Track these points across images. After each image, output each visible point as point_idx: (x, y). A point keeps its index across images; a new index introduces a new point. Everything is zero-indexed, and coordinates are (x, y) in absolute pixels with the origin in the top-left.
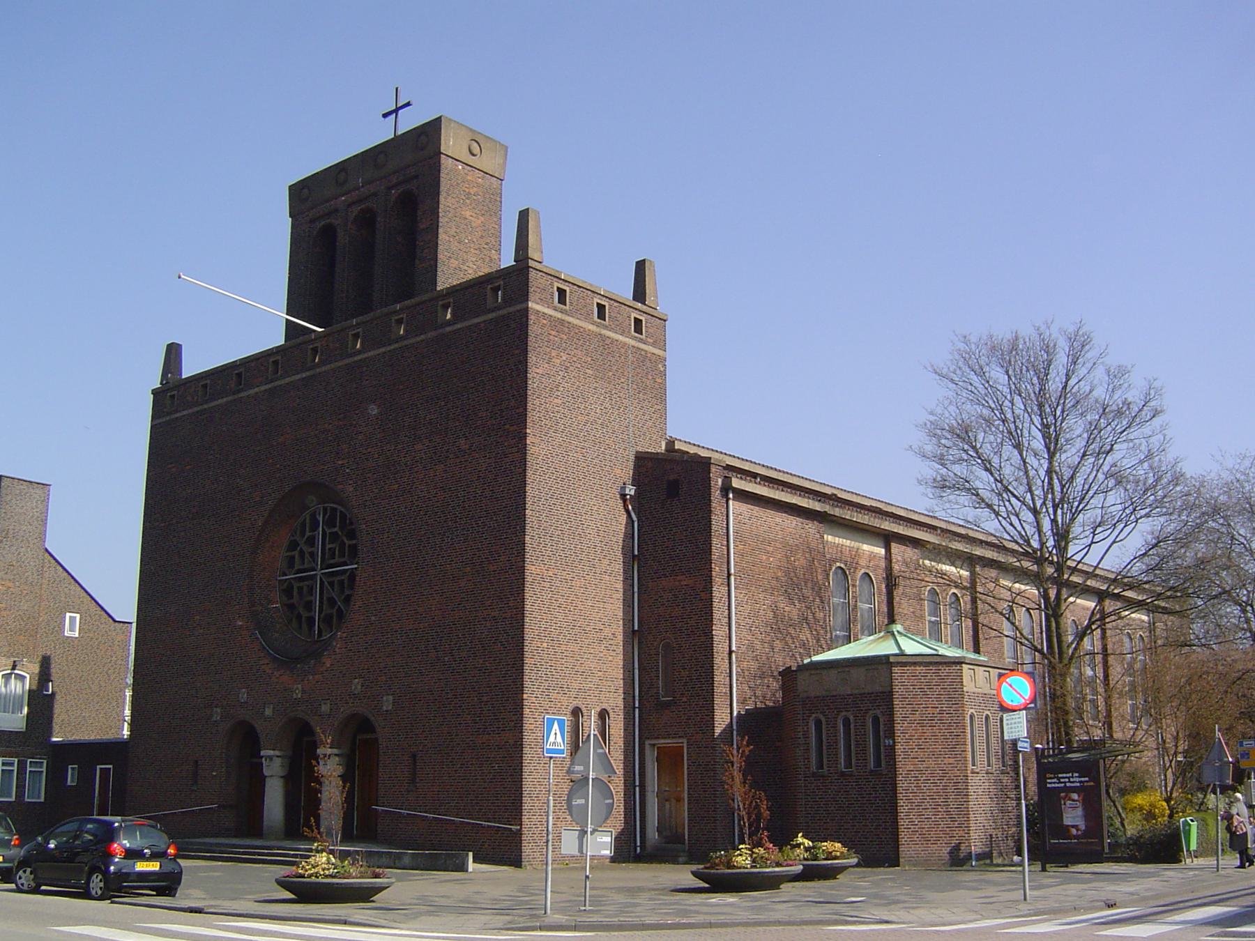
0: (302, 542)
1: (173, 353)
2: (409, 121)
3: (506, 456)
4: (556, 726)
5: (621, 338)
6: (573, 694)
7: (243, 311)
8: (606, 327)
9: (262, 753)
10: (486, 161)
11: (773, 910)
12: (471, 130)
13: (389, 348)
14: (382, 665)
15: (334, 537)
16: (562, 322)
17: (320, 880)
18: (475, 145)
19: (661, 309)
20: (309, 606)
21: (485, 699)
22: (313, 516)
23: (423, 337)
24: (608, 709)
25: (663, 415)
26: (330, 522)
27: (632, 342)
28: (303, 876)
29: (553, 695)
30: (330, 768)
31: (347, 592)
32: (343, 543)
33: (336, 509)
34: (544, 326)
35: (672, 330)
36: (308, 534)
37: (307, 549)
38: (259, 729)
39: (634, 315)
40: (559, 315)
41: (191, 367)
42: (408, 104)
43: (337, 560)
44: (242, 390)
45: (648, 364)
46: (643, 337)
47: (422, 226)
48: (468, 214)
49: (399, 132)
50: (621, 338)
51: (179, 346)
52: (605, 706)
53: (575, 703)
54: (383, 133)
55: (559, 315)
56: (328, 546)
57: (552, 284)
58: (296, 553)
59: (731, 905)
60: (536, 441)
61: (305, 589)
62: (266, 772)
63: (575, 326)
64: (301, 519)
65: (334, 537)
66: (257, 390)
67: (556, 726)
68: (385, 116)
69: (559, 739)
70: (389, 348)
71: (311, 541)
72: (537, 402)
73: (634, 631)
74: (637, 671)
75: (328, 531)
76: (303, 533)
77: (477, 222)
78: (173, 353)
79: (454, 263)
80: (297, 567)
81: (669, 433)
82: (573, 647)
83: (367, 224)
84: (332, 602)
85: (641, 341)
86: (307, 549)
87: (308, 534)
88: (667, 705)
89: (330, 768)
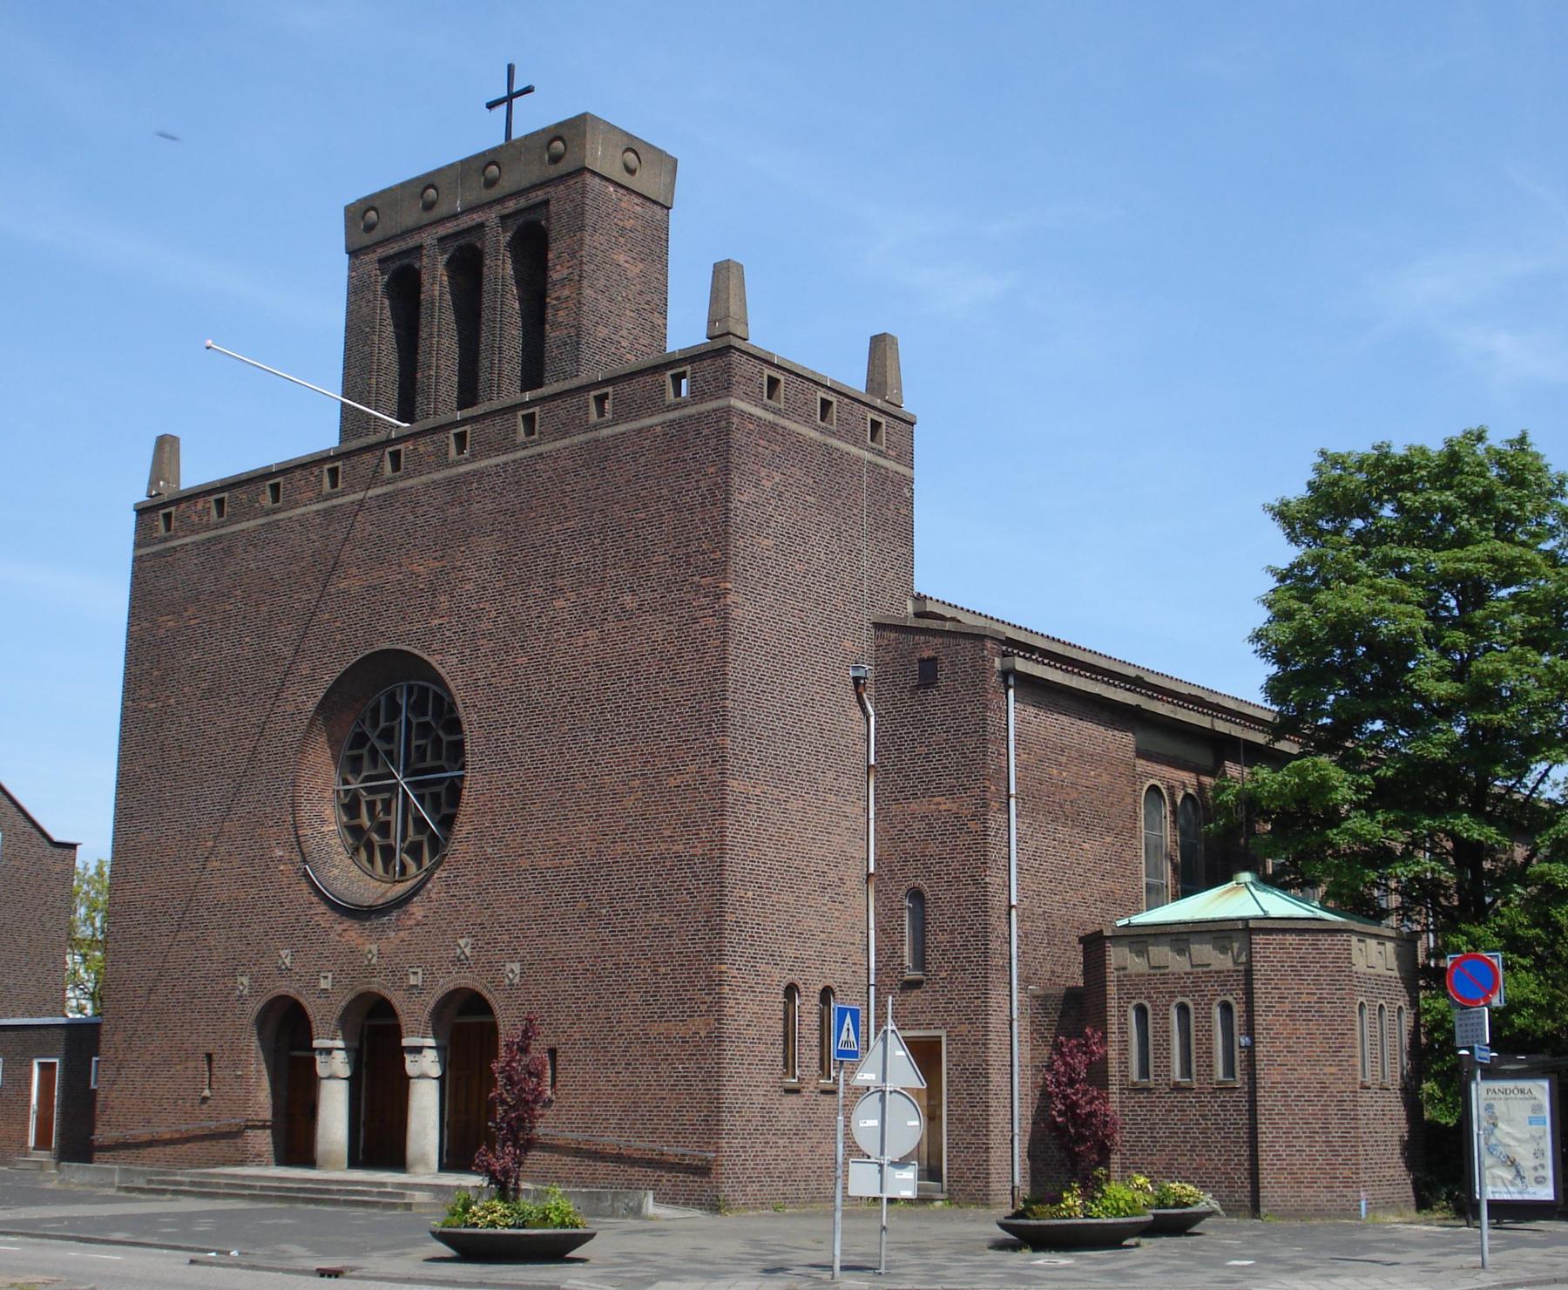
0: (373, 737)
1: (166, 448)
2: (531, 118)
3: (695, 621)
4: (848, 1020)
5: (853, 450)
6: (787, 964)
7: (275, 385)
8: (833, 434)
9: (316, 1043)
10: (643, 181)
11: (1136, 1276)
12: (627, 134)
13: (511, 457)
14: (504, 919)
15: (425, 729)
16: (774, 426)
17: (499, 1230)
18: (631, 156)
19: (908, 407)
20: (384, 829)
21: (662, 970)
22: (392, 698)
23: (566, 442)
24: (834, 986)
25: (908, 562)
26: (418, 707)
27: (868, 456)
28: (475, 1225)
29: (762, 967)
30: (425, 1068)
31: (445, 810)
32: (438, 740)
33: (427, 689)
34: (750, 432)
35: (923, 440)
36: (382, 724)
37: (381, 746)
38: (309, 1011)
39: (871, 415)
40: (770, 417)
41: (194, 473)
42: (528, 90)
43: (429, 763)
44: (279, 510)
45: (889, 487)
46: (883, 448)
47: (555, 276)
48: (621, 258)
49: (516, 134)
50: (853, 450)
51: (174, 441)
52: (829, 982)
53: (790, 978)
54: (487, 134)
55: (770, 417)
56: (414, 743)
57: (761, 373)
58: (365, 751)
59: (1067, 1268)
60: (740, 600)
61: (379, 807)
62: (321, 1070)
63: (792, 433)
64: (371, 703)
65: (425, 729)
66: (303, 510)
67: (848, 1020)
68: (491, 106)
69: (852, 1038)
70: (511, 457)
71: (388, 735)
72: (741, 543)
73: (869, 875)
74: (872, 933)
75: (414, 721)
76: (375, 724)
77: (634, 270)
78: (166, 448)
79: (603, 332)
80: (442, 789)
81: (916, 590)
82: (788, 897)
83: (484, 274)
84: (421, 824)
85: (880, 453)
86: (381, 746)
87: (382, 724)
88: (916, 984)
89: (425, 1068)
